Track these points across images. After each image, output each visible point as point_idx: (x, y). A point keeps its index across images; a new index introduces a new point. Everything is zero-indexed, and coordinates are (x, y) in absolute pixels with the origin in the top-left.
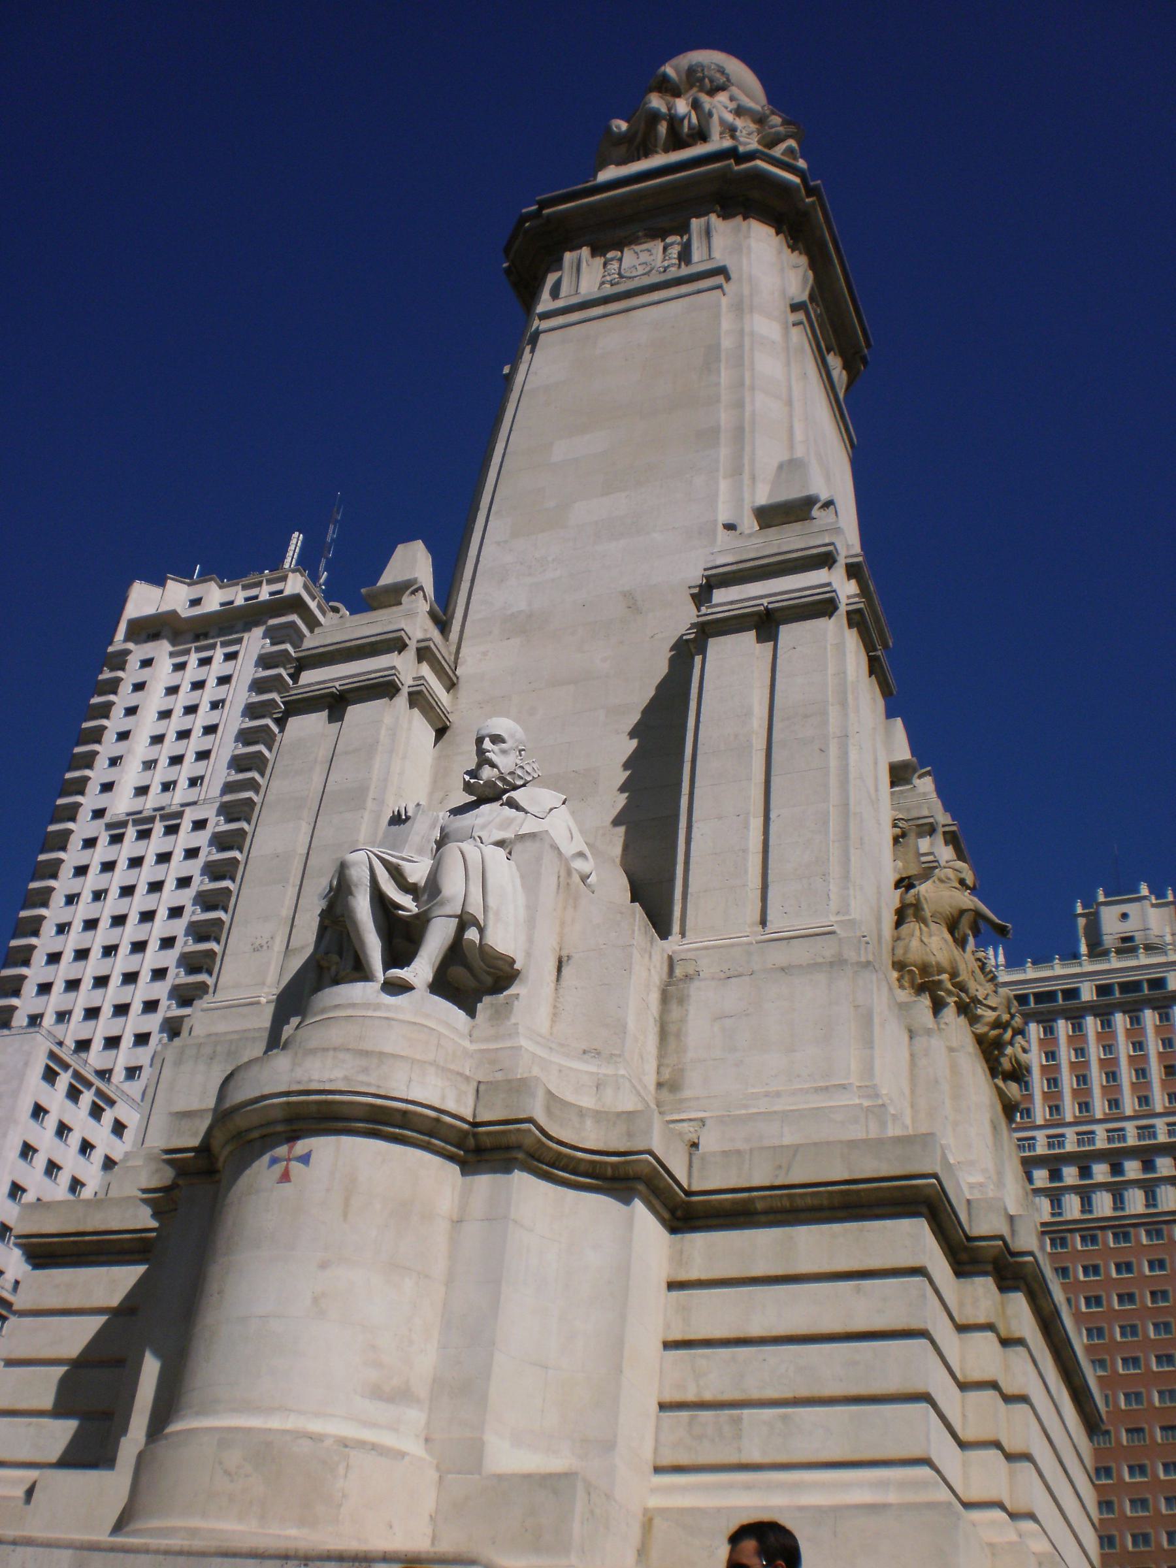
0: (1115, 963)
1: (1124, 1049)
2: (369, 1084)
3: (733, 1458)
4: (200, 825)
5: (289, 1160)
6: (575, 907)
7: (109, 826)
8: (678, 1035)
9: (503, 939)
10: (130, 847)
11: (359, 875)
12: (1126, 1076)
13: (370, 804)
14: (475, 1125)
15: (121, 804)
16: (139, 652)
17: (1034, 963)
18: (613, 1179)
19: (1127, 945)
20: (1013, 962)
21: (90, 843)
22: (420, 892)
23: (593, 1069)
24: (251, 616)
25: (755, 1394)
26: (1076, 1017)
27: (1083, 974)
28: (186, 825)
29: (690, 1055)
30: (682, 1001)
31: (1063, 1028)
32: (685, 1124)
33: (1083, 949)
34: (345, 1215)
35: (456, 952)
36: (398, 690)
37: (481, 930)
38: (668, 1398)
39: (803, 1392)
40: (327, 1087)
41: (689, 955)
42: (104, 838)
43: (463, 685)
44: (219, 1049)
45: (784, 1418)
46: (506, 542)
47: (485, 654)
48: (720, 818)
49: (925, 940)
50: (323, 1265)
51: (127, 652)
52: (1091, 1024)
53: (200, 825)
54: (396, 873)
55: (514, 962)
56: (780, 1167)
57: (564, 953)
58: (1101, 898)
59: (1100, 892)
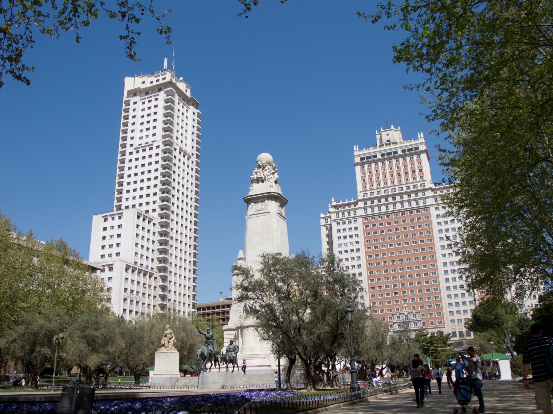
0: (385, 148)
1: (388, 170)
4: (158, 147)
7: (135, 149)
10: (141, 154)
12: (388, 176)
15: (136, 142)
16: (133, 100)
17: (366, 149)
19: (389, 143)
20: (361, 149)
21: (131, 153)
24: (159, 88)
26: (376, 162)
27: (377, 151)
28: (154, 147)
31: (373, 165)
33: (378, 144)
42: (134, 152)
51: (130, 100)
52: (380, 164)
53: (158, 147)
58: (382, 130)
59: (382, 129)
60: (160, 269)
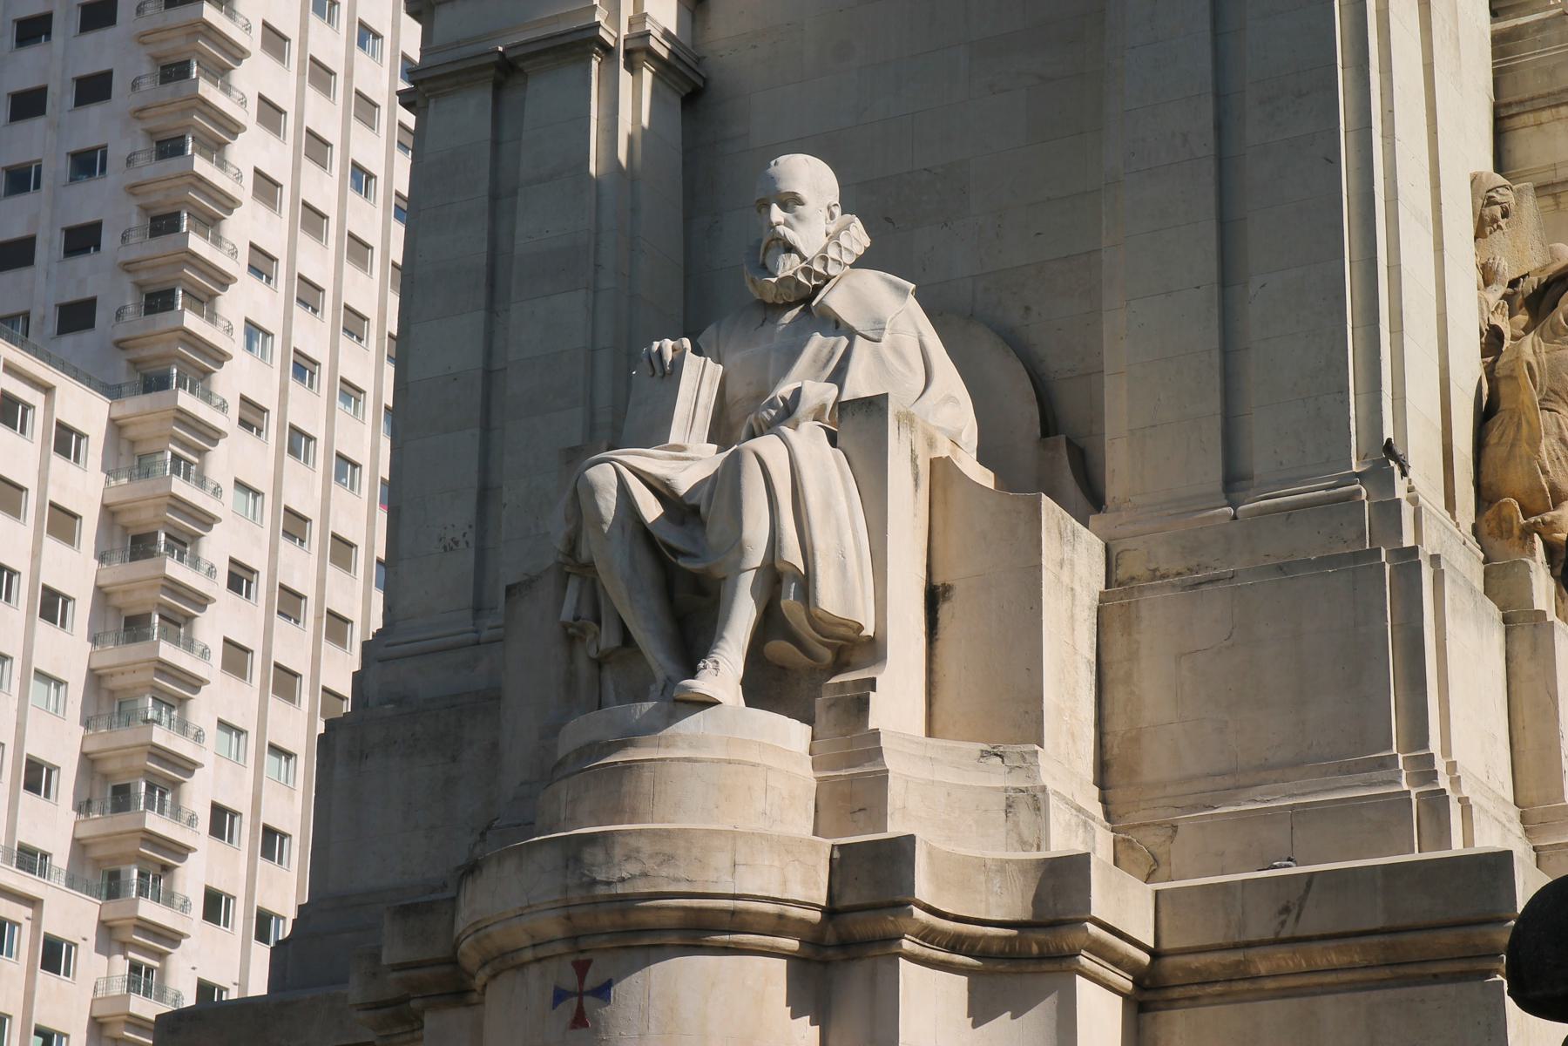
2: (677, 880)
5: (581, 995)
30: (1128, 628)
35: (770, 622)
37: (807, 584)
54: (662, 490)
55: (861, 628)
57: (938, 581)
60: (100, 872)
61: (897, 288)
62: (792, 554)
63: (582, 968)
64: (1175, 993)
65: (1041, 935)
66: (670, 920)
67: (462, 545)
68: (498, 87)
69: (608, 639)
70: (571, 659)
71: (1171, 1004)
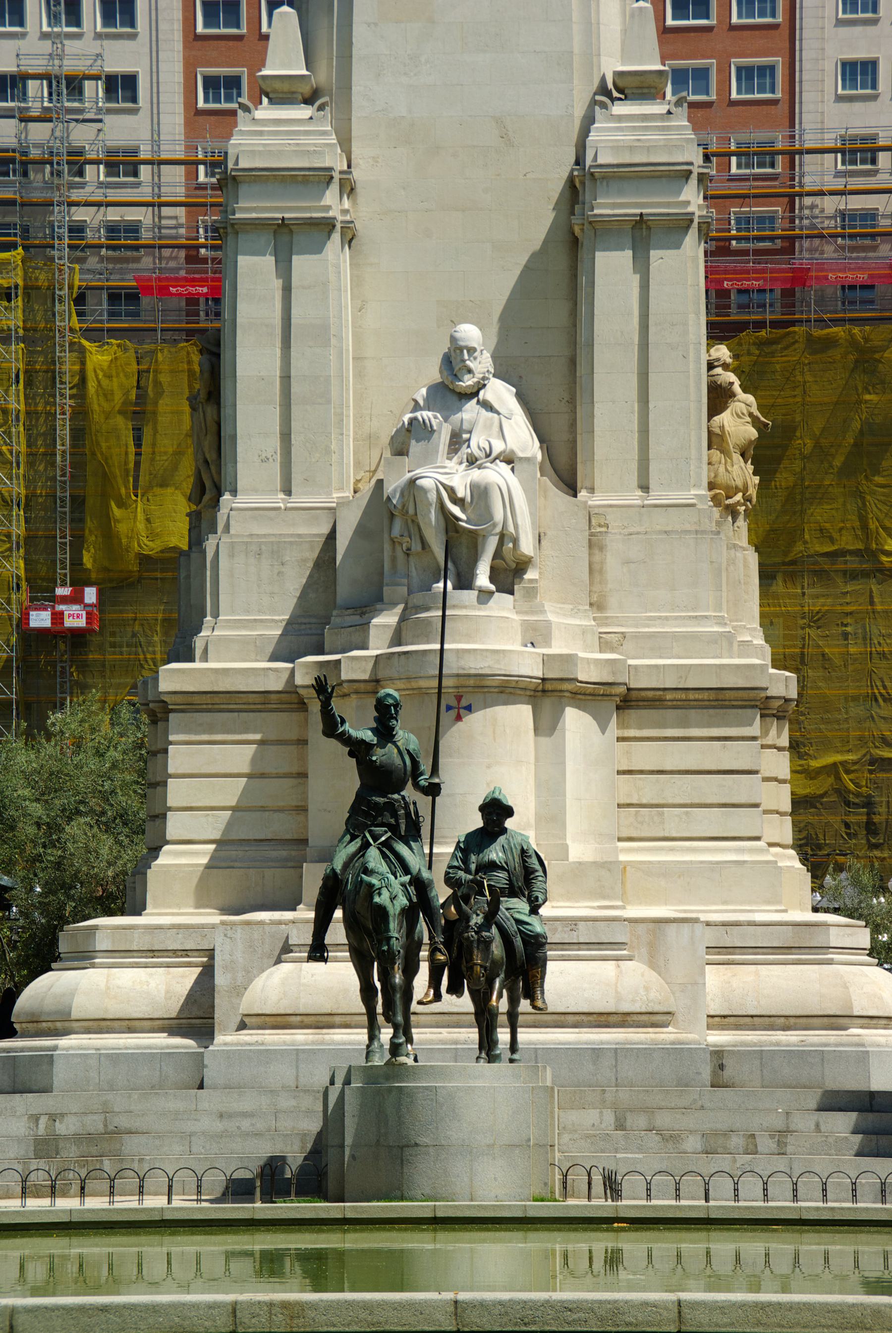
2: (501, 669)
3: (661, 834)
5: (459, 708)
6: (545, 497)
8: (601, 571)
9: (527, 546)
11: (432, 497)
13: (333, 341)
14: (543, 679)
18: (602, 695)
22: (466, 505)
23: (578, 622)
25: (670, 801)
29: (610, 586)
30: (601, 548)
32: (613, 635)
34: (495, 740)
35: (498, 554)
36: (334, 226)
37: (515, 541)
38: (622, 802)
39: (696, 801)
40: (481, 672)
41: (601, 510)
43: (359, 189)
44: (263, 547)
45: (687, 813)
46: (376, 24)
47: (375, 159)
48: (614, 402)
49: (729, 469)
50: (489, 767)
54: (451, 491)
56: (681, 677)
57: (542, 530)
61: (509, 390)
62: (511, 529)
63: (459, 698)
64: (633, 703)
65: (606, 687)
66: (494, 684)
67: (271, 460)
68: (275, 232)
69: (416, 547)
70: (394, 549)
71: (629, 707)
